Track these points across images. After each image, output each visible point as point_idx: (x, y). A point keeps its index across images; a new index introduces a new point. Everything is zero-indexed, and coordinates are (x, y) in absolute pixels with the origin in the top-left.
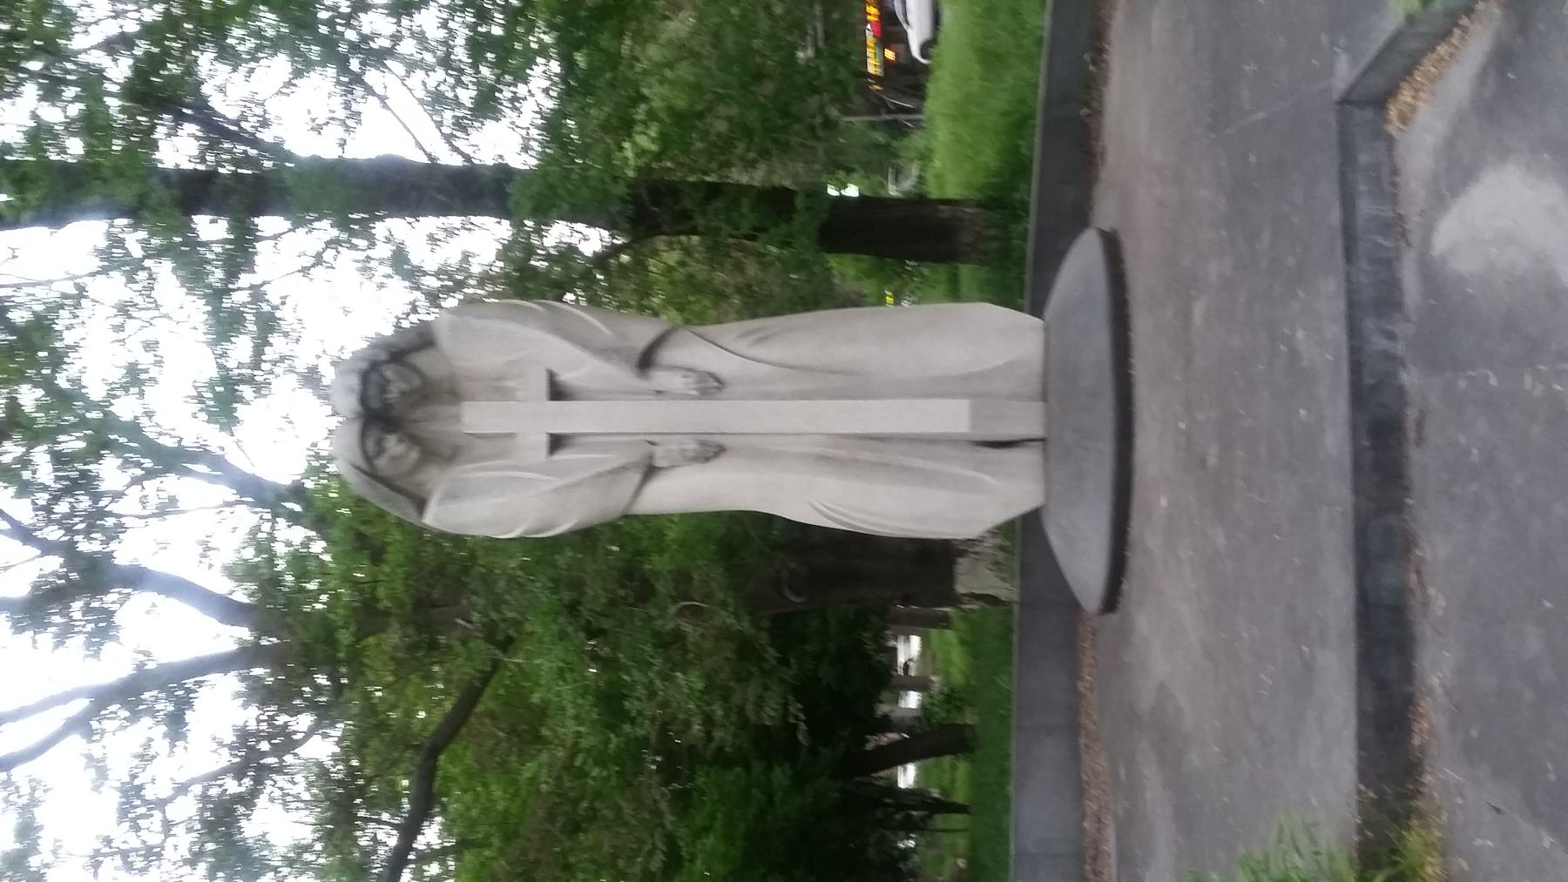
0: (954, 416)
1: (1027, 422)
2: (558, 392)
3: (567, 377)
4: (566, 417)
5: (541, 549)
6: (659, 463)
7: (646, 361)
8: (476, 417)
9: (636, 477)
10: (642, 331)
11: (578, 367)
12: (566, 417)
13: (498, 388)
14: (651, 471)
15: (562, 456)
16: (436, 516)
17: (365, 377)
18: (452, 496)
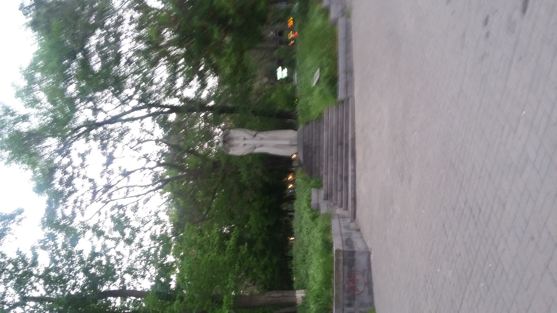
0: (287, 142)
1: (295, 143)
2: (245, 139)
3: (246, 137)
4: (246, 142)
5: (241, 157)
6: (256, 147)
7: (255, 136)
8: (235, 142)
9: (254, 148)
10: (254, 133)
11: (247, 136)
12: (246, 142)
13: (237, 138)
14: (255, 148)
15: (245, 146)
16: (231, 153)
17: (224, 137)
18: (233, 150)
